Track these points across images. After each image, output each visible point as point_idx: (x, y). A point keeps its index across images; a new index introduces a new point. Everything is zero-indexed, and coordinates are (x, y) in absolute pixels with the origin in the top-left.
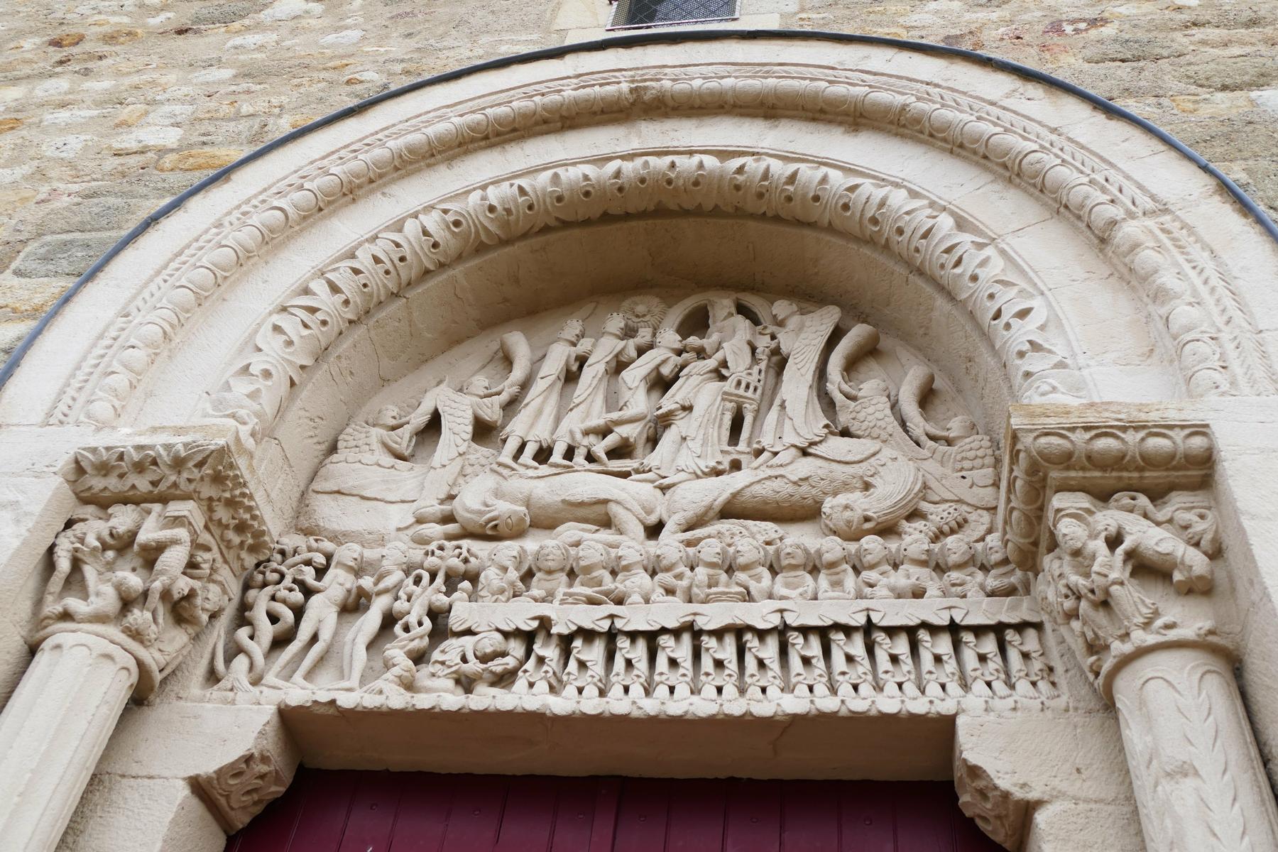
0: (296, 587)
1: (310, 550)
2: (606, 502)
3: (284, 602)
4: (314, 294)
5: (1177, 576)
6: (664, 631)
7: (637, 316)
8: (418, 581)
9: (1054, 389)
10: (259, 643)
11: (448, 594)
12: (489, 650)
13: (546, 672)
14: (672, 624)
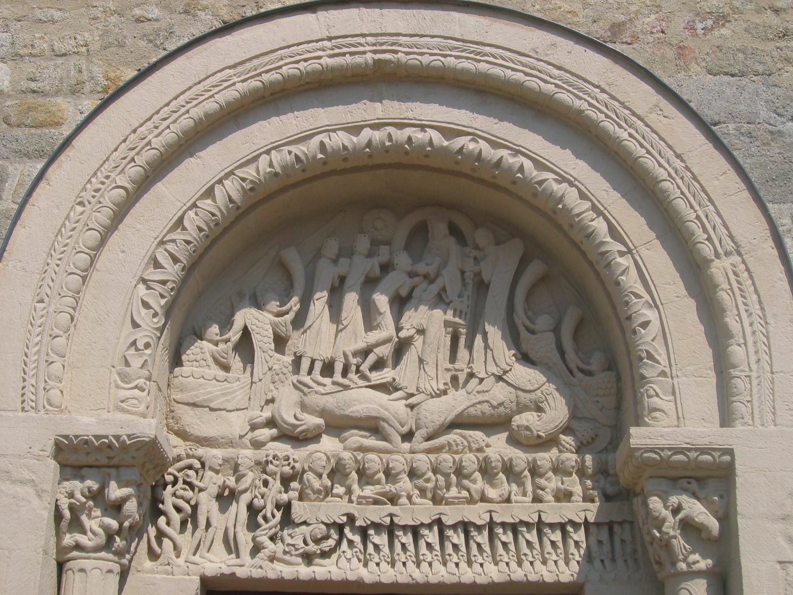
0: (187, 487)
1: (188, 456)
2: (377, 419)
3: (182, 498)
4: (163, 268)
5: (703, 535)
6: (422, 524)
7: (377, 230)
8: (266, 483)
9: (657, 395)
10: (175, 529)
11: (286, 492)
12: (319, 536)
13: (356, 552)
14: (427, 521)
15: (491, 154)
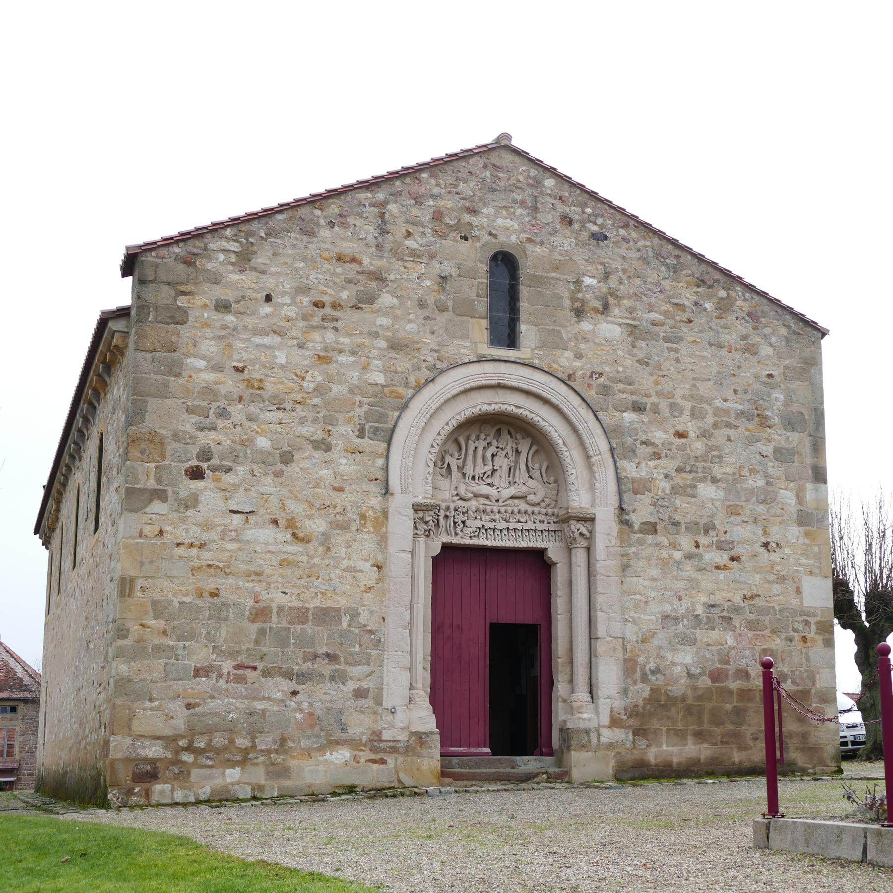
15: (530, 416)
